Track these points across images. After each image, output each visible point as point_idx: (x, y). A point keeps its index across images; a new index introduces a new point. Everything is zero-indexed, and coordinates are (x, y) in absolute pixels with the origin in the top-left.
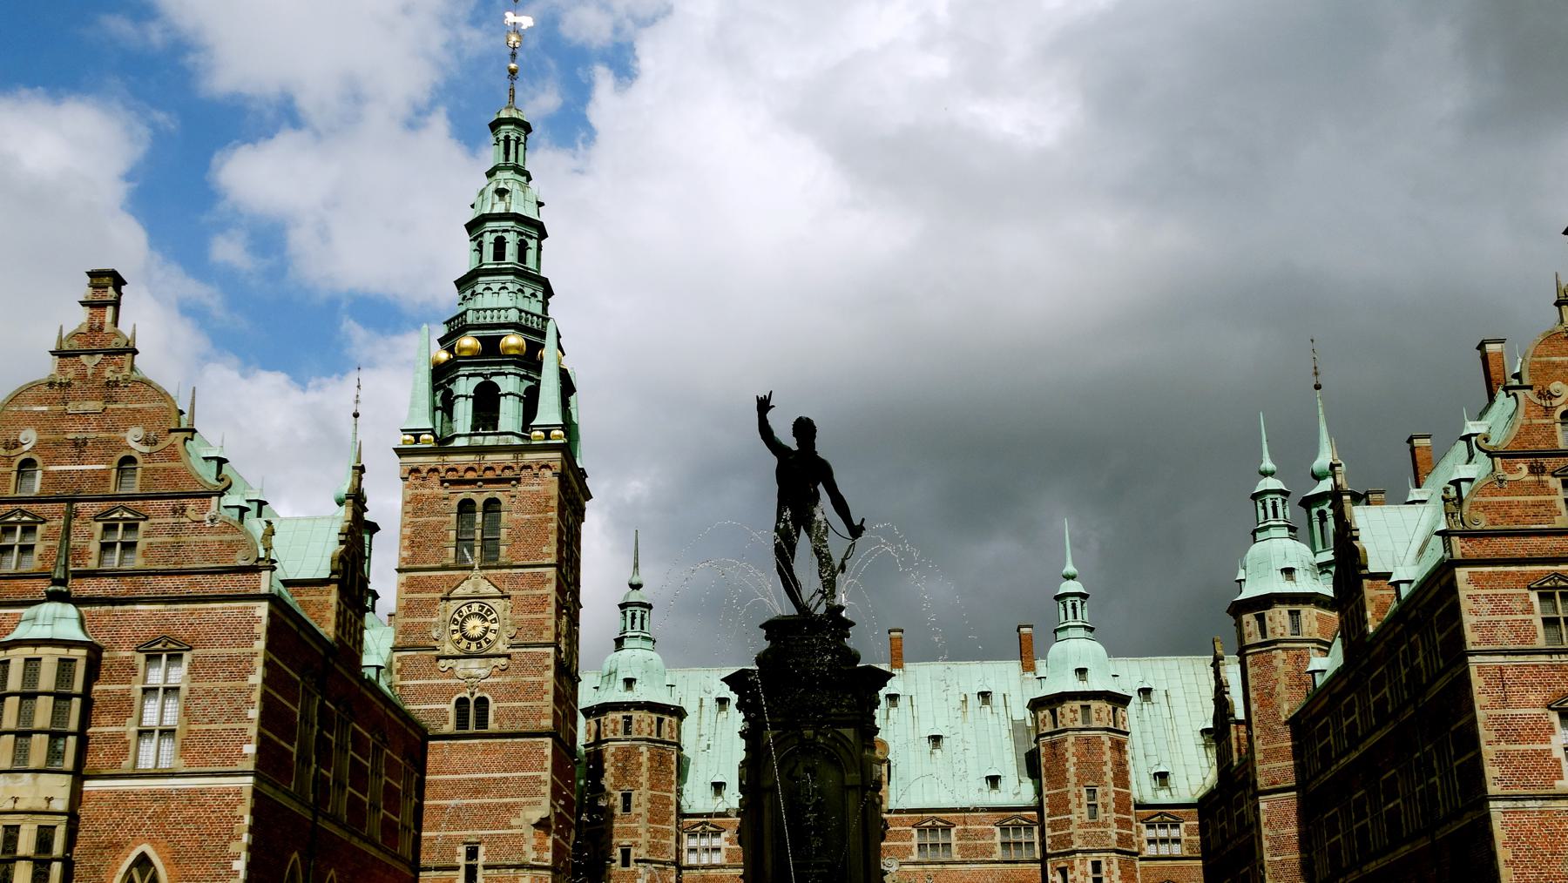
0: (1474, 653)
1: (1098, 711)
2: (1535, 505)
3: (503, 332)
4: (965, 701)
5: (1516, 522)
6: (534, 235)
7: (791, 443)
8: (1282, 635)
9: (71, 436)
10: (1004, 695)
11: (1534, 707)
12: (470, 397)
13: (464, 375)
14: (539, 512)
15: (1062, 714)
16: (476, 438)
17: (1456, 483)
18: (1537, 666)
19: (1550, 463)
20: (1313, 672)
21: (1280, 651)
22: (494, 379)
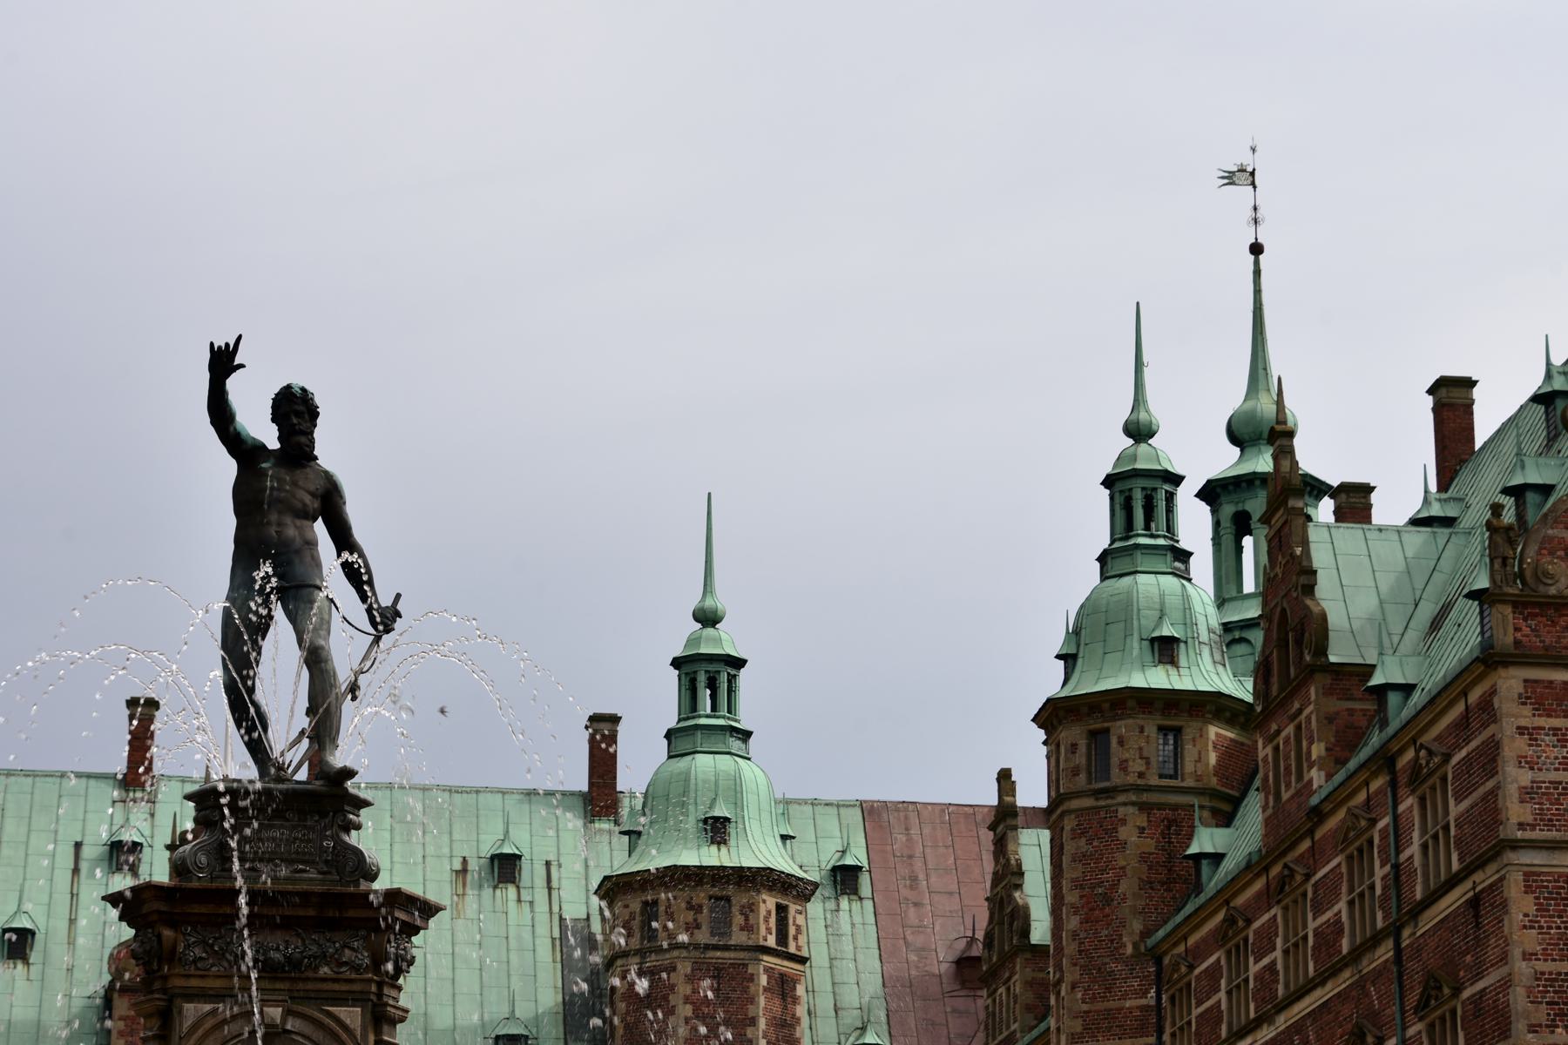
0: (1515, 845)
4: (464, 871)
7: (269, 436)
8: (1141, 775)
10: (548, 864)
17: (1517, 492)
20: (1198, 857)
21: (1131, 809)
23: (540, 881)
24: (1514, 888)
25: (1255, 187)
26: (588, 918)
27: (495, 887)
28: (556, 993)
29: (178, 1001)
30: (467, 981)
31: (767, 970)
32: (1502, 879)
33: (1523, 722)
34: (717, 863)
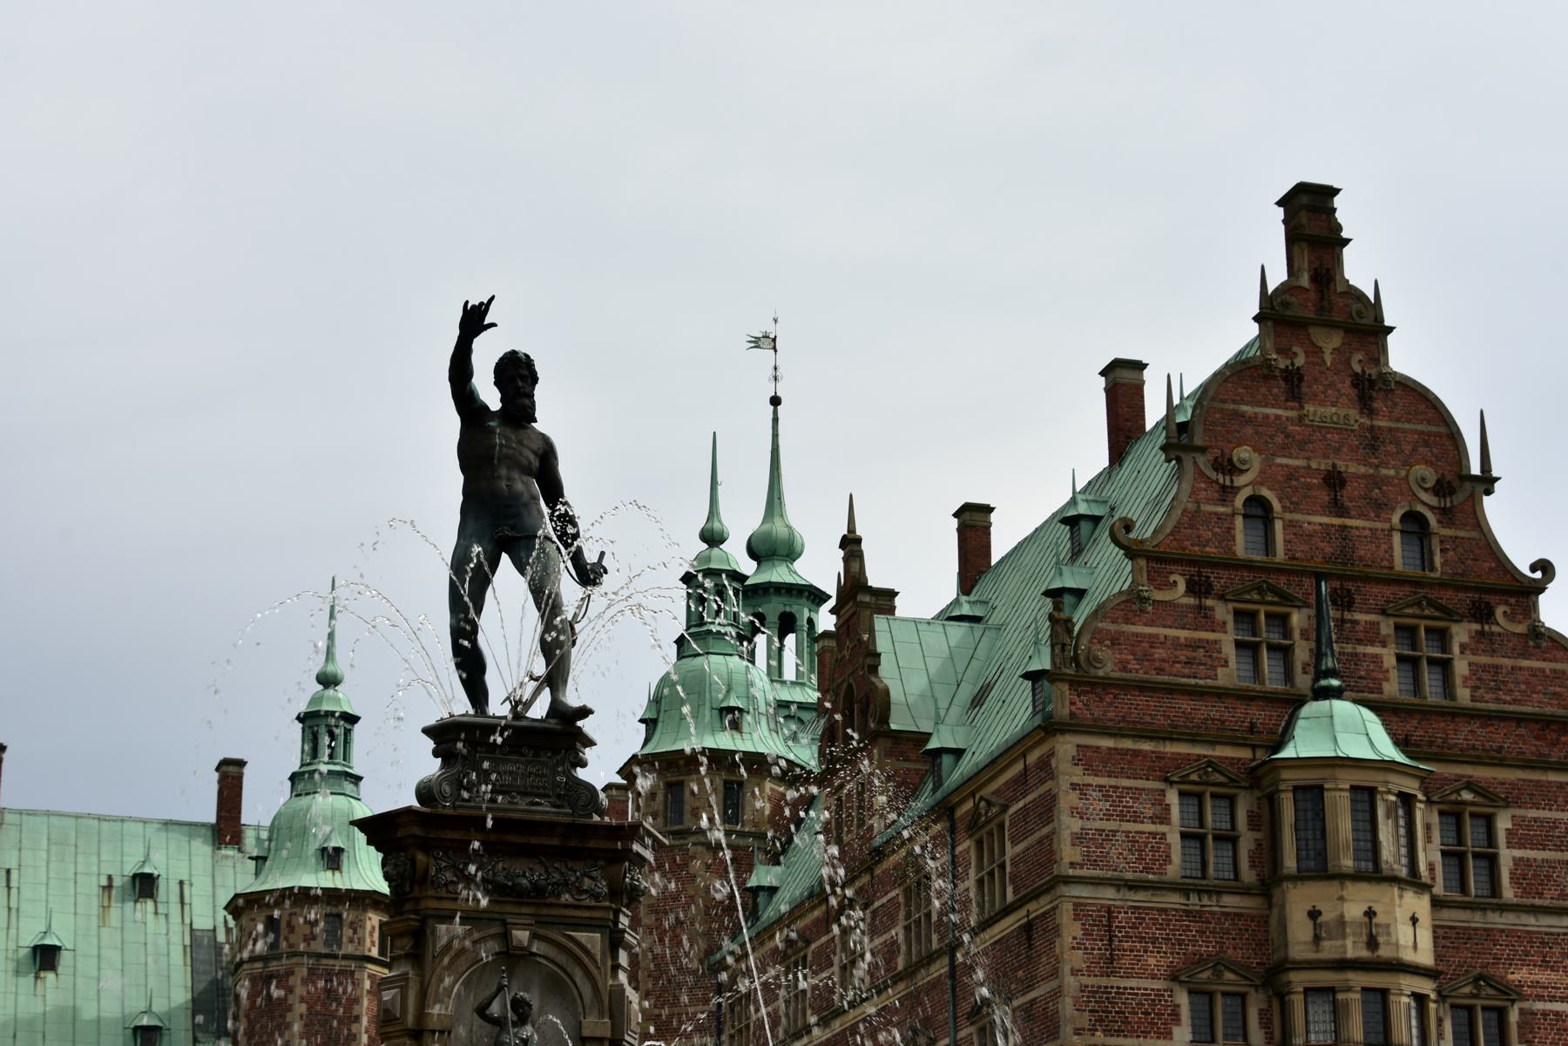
0: (1068, 880)
1: (356, 926)
2: (1193, 645)
4: (109, 887)
5: (1160, 671)
10: (181, 883)
11: (1154, 977)
15: (289, 924)
18: (1165, 910)
19: (1219, 579)
23: (175, 898)
24: (1066, 915)
25: (776, 351)
26: (214, 930)
27: (136, 901)
28: (186, 991)
29: (431, 922)
30: (111, 982)
31: (370, 976)
32: (1054, 909)
33: (1076, 780)
34: (332, 886)
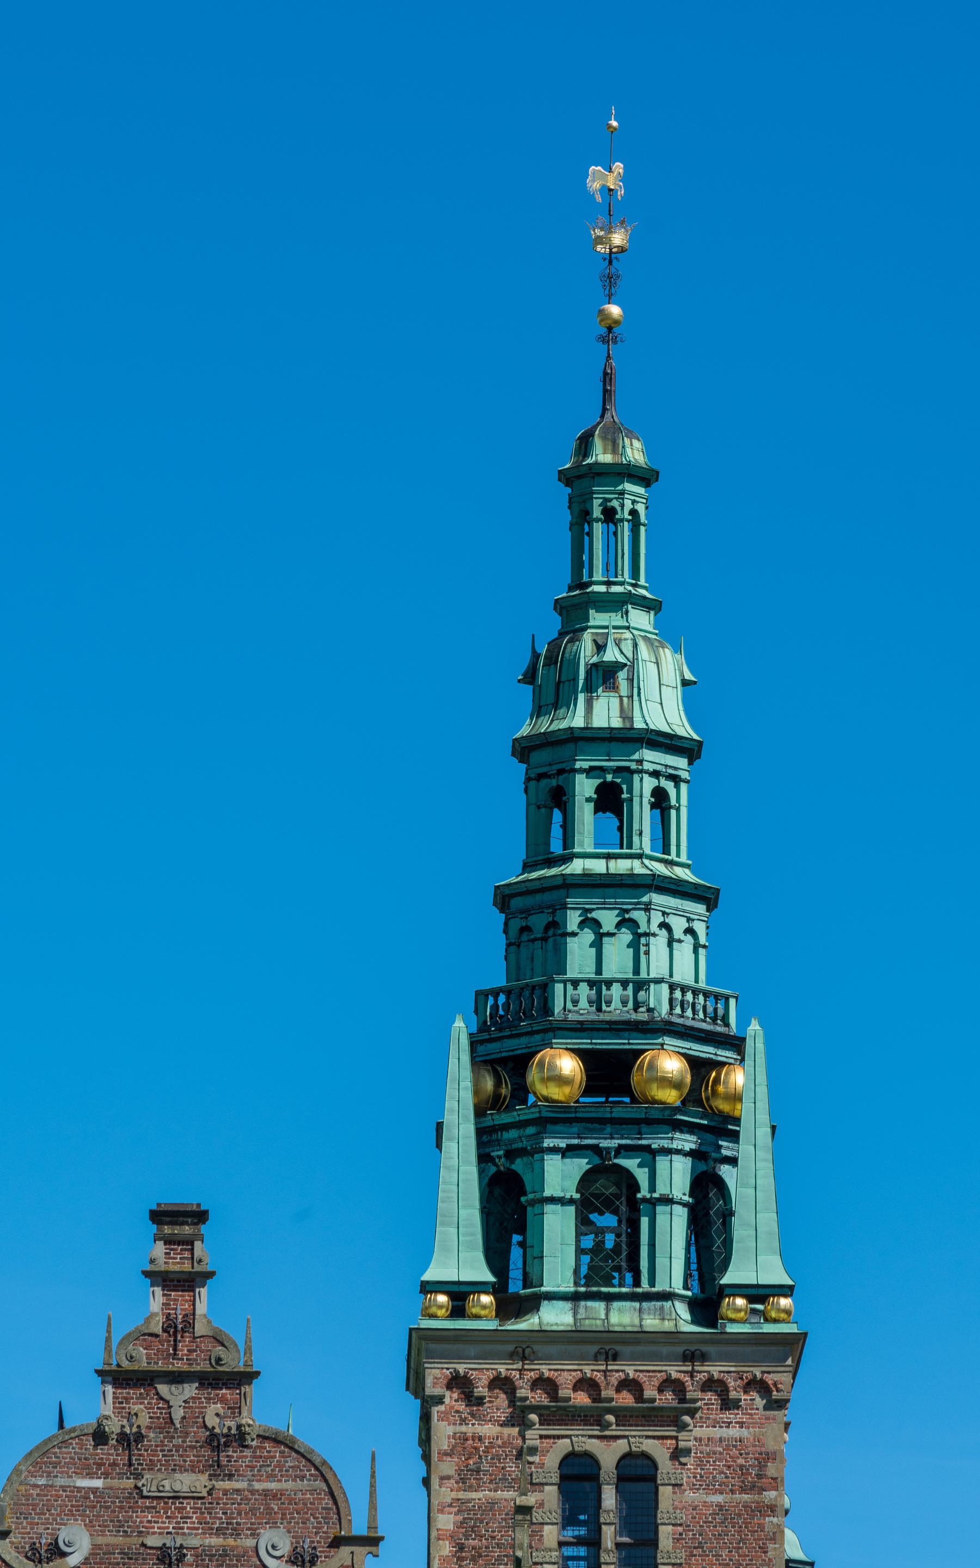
3: (636, 1043)
6: (684, 775)
9: (152, 1541)
12: (571, 1201)
13: (554, 1150)
14: (743, 1490)
16: (590, 1304)
22: (631, 1164)
